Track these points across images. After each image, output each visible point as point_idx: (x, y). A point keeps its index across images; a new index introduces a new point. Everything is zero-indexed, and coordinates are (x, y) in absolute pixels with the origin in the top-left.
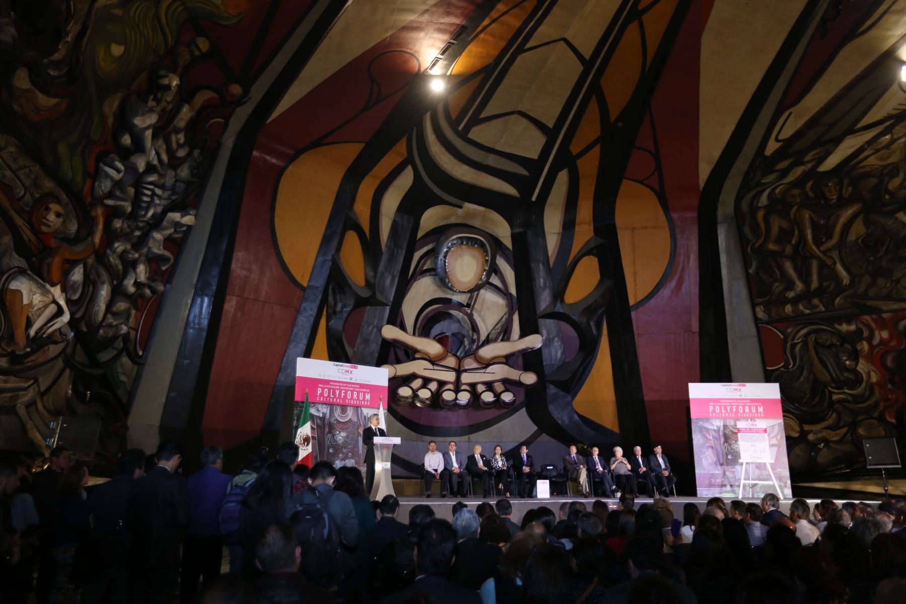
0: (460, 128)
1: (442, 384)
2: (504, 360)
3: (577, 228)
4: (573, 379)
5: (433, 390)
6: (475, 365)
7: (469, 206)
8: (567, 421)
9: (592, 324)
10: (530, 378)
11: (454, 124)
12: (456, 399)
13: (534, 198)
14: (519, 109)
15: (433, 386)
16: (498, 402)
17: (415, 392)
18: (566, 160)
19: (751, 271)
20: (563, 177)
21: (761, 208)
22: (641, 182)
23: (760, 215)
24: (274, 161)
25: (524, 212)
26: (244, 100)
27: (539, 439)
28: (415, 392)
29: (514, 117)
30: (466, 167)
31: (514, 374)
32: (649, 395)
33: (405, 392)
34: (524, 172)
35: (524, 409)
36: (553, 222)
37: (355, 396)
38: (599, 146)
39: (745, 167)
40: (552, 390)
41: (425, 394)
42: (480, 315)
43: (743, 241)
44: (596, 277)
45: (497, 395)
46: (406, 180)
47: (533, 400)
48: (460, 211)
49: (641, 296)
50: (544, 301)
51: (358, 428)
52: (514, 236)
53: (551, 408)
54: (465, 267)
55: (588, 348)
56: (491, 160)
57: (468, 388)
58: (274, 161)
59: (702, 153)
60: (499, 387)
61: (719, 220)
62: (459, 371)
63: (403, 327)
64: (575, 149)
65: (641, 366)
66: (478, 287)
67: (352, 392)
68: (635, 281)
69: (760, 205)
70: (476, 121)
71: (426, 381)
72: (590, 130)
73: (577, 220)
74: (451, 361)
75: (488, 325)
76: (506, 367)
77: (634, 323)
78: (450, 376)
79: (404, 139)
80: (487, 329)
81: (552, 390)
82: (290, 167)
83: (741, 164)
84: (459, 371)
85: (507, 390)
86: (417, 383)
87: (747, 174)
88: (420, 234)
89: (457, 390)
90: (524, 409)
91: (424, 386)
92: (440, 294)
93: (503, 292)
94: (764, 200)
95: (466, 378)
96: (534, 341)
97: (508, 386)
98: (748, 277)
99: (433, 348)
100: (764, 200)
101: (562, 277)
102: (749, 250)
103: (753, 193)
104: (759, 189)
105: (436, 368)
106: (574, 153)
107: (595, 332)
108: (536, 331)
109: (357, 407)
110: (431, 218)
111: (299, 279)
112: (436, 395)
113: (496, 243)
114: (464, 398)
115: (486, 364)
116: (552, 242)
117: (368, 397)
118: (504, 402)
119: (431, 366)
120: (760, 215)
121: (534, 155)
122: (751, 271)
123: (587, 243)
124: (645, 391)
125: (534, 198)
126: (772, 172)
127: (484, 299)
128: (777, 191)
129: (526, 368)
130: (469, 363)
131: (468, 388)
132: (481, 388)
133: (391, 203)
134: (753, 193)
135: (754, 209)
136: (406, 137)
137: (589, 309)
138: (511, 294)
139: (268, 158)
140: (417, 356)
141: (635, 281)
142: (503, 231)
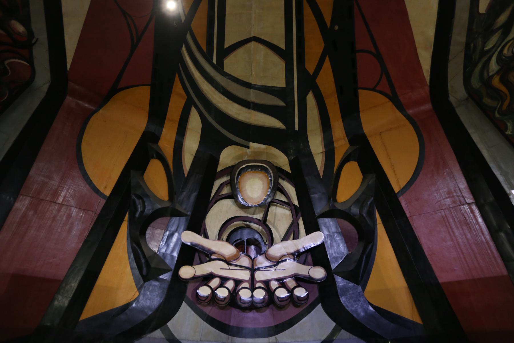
0: (215, 61)
1: (238, 282)
3: (336, 145)
4: (359, 268)
5: (230, 289)
6: (268, 264)
7: (253, 145)
8: (362, 314)
9: (365, 215)
10: (318, 273)
11: (208, 57)
12: (252, 296)
13: (297, 128)
14: (253, 35)
15: (230, 285)
16: (292, 299)
17: (213, 291)
18: (308, 83)
19: (508, 132)
20: (310, 99)
21: (493, 76)
22: (374, 90)
23: (496, 82)
24: (86, 105)
25: (290, 139)
26: (33, 41)
28: (213, 291)
29: (253, 45)
30: (236, 106)
31: (303, 270)
33: (204, 291)
34: (282, 104)
35: (320, 305)
36: (316, 145)
38: (327, 58)
39: (463, 39)
40: (340, 281)
41: (222, 293)
42: (274, 227)
43: (487, 112)
44: (358, 176)
45: (291, 291)
46: (195, 122)
47: (325, 294)
48: (248, 151)
49: (403, 184)
50: (320, 206)
52: (291, 163)
53: (343, 300)
54: (254, 189)
56: (252, 96)
57: (262, 286)
58: (86, 105)
59: (418, 39)
60: (291, 283)
61: (455, 105)
62: (253, 270)
63: (206, 236)
64: (310, 67)
66: (270, 204)
68: (394, 171)
69: (491, 74)
70: (225, 52)
71: (224, 280)
72: (315, 45)
73: (334, 139)
74: (245, 261)
75: (281, 233)
78: (245, 275)
79: (177, 78)
80: (280, 236)
81: (340, 281)
82: (101, 111)
83: (459, 37)
84: (253, 270)
85: (298, 286)
86: (215, 282)
87: (467, 45)
88: (219, 169)
89: (253, 288)
90: (320, 305)
91: (221, 285)
92: (241, 213)
93: (288, 204)
94: (494, 66)
95: (260, 276)
97: (301, 283)
98: (507, 138)
99: (228, 249)
100: (494, 66)
101: (332, 179)
102: (497, 115)
103: (480, 66)
104: (485, 59)
105: (231, 267)
106: (311, 73)
108: (318, 229)
110: (228, 157)
111: (101, 189)
112: (234, 294)
113: (279, 172)
114: (260, 294)
115: (277, 262)
116: (319, 161)
119: (226, 266)
120: (496, 82)
121: (282, 83)
122: (508, 132)
123: (345, 153)
124: (437, 272)
125: (297, 128)
126: (493, 32)
127: (275, 213)
128: (505, 51)
129: (315, 264)
130: (262, 261)
131: (262, 286)
132: (274, 285)
133: (192, 144)
134: (480, 66)
135: (487, 83)
136: (177, 75)
137: (359, 200)
138: (295, 206)
139: (80, 102)
140: (213, 257)
141: (394, 171)
142: (282, 160)
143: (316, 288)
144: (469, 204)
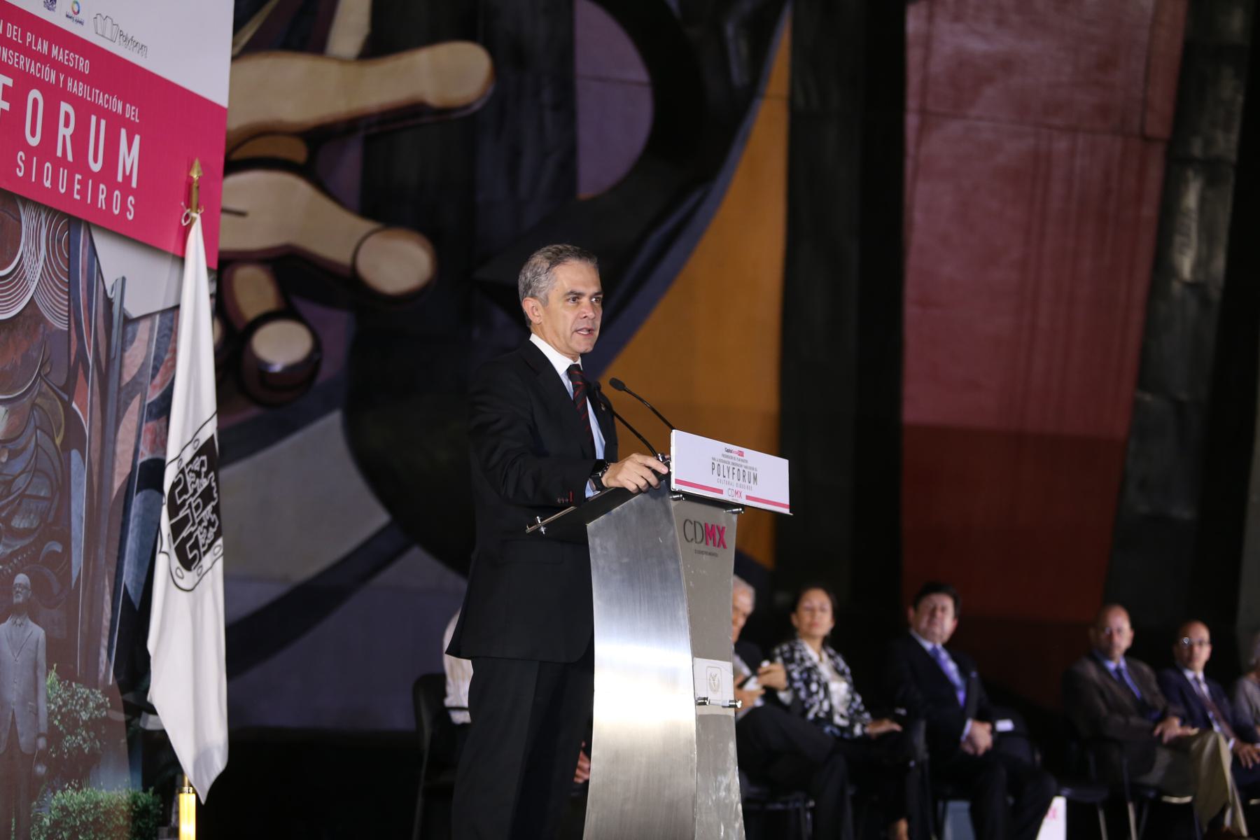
2: (299, 153)
27: (390, 575)
31: (331, 231)
32: (921, 403)
37: (65, 132)
51: (69, 388)
55: (689, 145)
65: (914, 262)
67: (54, 95)
76: (300, 189)
77: (914, 56)
85: (285, 312)
90: (334, 420)
96: (451, 72)
107: (739, 76)
109: (73, 224)
117: (129, 158)
118: (262, 368)
129: (381, 206)
143: (339, 324)
144: (1146, 139)
